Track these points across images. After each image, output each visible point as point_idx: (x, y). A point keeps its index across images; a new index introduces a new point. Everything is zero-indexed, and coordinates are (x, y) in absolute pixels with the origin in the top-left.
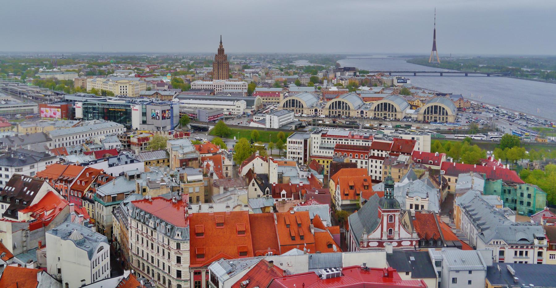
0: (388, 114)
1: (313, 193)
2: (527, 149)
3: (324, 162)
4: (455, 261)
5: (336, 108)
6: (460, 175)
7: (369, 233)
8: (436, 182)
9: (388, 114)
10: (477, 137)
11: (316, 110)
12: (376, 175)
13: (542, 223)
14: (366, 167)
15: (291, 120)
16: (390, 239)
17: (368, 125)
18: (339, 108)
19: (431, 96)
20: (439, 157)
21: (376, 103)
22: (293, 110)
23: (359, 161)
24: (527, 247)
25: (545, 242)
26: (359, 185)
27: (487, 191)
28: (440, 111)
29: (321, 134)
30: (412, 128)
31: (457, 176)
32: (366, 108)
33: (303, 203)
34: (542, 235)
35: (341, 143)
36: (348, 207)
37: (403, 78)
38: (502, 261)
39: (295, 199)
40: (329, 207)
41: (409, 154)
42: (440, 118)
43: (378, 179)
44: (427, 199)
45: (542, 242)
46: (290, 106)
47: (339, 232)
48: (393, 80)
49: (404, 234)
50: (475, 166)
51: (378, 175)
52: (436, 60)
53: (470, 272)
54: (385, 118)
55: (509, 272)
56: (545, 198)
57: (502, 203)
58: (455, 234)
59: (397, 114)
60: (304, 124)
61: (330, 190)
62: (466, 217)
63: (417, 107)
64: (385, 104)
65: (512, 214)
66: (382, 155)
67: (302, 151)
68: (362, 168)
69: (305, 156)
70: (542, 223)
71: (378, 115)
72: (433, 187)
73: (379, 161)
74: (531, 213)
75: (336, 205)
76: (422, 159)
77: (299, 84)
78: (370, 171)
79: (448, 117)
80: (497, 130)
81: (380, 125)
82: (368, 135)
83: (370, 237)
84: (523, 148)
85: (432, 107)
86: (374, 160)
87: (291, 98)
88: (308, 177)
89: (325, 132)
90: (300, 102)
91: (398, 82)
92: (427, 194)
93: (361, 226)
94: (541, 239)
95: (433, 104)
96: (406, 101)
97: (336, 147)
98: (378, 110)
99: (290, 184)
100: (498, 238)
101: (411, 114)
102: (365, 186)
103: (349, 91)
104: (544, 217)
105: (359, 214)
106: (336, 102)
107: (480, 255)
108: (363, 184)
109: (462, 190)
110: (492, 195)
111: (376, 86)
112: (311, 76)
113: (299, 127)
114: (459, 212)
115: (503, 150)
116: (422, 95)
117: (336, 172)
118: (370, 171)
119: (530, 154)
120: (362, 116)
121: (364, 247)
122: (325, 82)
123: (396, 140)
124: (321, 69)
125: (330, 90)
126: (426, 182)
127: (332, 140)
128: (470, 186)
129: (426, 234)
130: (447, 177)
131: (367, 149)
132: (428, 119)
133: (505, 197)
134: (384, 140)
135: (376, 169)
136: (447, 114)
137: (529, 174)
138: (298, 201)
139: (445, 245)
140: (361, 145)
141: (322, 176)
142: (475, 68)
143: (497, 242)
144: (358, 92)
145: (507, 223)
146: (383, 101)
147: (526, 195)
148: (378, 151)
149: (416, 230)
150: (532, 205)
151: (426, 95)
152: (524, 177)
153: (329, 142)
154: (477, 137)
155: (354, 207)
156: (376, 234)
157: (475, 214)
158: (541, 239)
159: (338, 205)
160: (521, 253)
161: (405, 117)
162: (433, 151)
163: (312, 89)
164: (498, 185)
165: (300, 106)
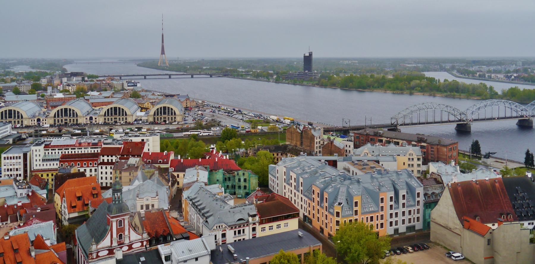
0: (118, 118)
1: (34, 212)
2: (243, 140)
3: (48, 175)
4: (183, 252)
5: (62, 115)
6: (187, 170)
7: (97, 242)
8: (166, 179)
9: (118, 118)
10: (204, 133)
11: (39, 120)
12: (106, 181)
13: (255, 202)
14: (96, 175)
15: (8, 133)
16: (121, 244)
17: (97, 131)
18: (66, 115)
19: (160, 97)
20: (168, 156)
21: (105, 108)
22: (10, 122)
23: (88, 169)
24: (244, 226)
25: (257, 218)
26: (88, 194)
27: (210, 182)
28: (169, 112)
29: (43, 145)
30: (143, 130)
31: (184, 171)
32: (96, 114)
33: (22, 224)
34: (255, 213)
35: (67, 153)
36: (77, 220)
37: (133, 81)
38: (224, 242)
39: (11, 222)
40: (53, 224)
41: (139, 156)
42: (168, 118)
43: (109, 185)
44: (157, 197)
45: (255, 218)
46: (6, 117)
47: (65, 248)
48: (123, 84)
49: (134, 236)
50: (200, 160)
51: (109, 181)
52: (164, 63)
53: (197, 259)
54: (116, 122)
55: (229, 251)
56: (257, 180)
57: (223, 190)
58: (183, 226)
59: (127, 117)
60: (24, 136)
61: (55, 205)
62: (192, 208)
63: (147, 109)
64: (115, 108)
65: (231, 199)
66: (112, 160)
67: (22, 166)
68: (91, 176)
69: (25, 171)
70: (255, 202)
71: (108, 120)
72: (163, 185)
73: (109, 167)
74: (247, 194)
75: (63, 220)
76: (152, 159)
77: (17, 92)
78: (100, 178)
79: (176, 117)
80: (219, 125)
81: (111, 130)
82: (96, 141)
83: (99, 247)
84: (239, 139)
85: (161, 108)
86: (104, 167)
87: (7, 108)
88: (28, 195)
89: (48, 143)
90: (18, 112)
91: (128, 86)
92: (157, 192)
93: (90, 237)
94: (254, 216)
95: (162, 105)
96: (136, 104)
97: (61, 158)
98: (108, 115)
99: (6, 206)
100: (220, 223)
101: (141, 116)
102: (93, 195)
103: (77, 97)
104: (256, 197)
105: (87, 224)
106: (62, 110)
107: (205, 241)
108: (92, 193)
109: (189, 184)
110: (215, 184)
111: (106, 90)
112: (32, 82)
113: (18, 140)
114: (187, 205)
115: (223, 142)
116: (152, 97)
117: (61, 184)
118: (100, 178)
119: (246, 143)
120: (91, 122)
121: (93, 259)
122: (50, 89)
123: (126, 143)
124: (44, 75)
125: (55, 97)
126: (156, 181)
127: (57, 151)
128: (196, 180)
129: (157, 232)
130: (175, 174)
131: (95, 156)
132: (158, 120)
133: (226, 184)
134: (114, 144)
135: (106, 176)
136: (175, 114)
137: (245, 161)
138: (15, 223)
139: (174, 239)
140: (89, 152)
141: (45, 191)
142: (200, 70)
143: (219, 227)
144: (86, 97)
145: (227, 208)
146: (113, 106)
147: (242, 180)
148: (108, 156)
149: (147, 230)
150: (247, 188)
151: (155, 97)
152: (241, 165)
153: (54, 153)
154: (204, 133)
155: (82, 219)
156: (106, 242)
157: (201, 205)
158: (254, 216)
159: (65, 219)
160: (239, 232)
161: (136, 120)
162: (162, 150)
163: (34, 97)
164: (219, 175)
165: (18, 117)
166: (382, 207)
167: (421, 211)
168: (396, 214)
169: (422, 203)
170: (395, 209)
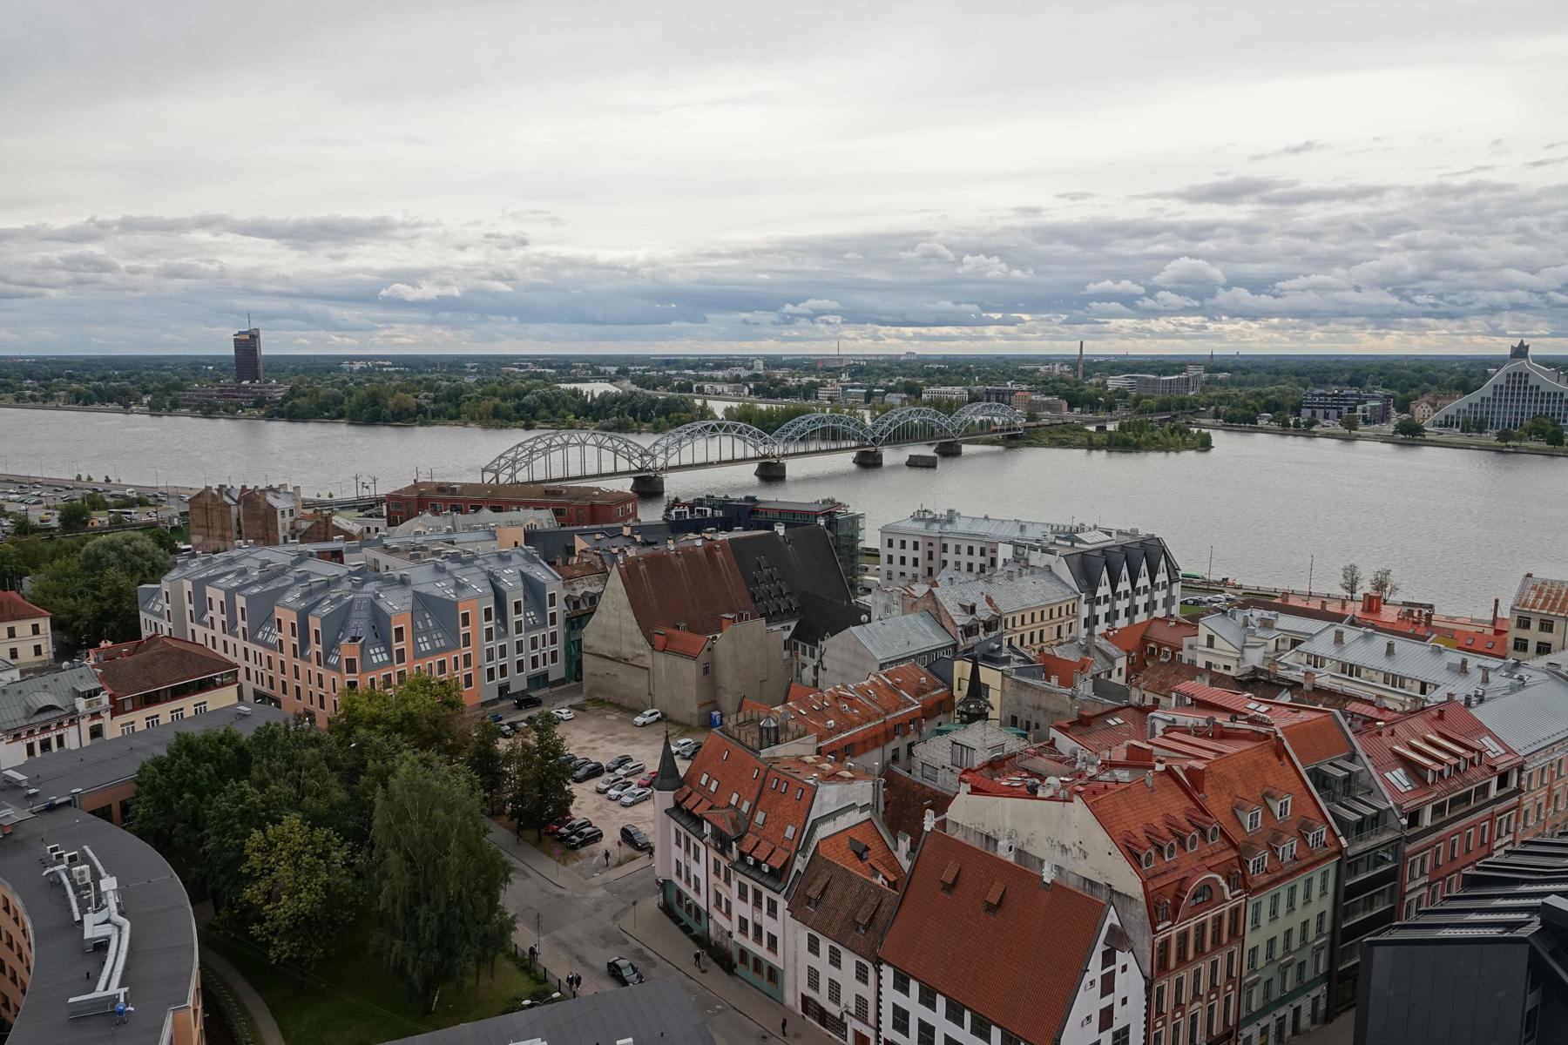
166: (467, 636)
167: (560, 638)
168: (503, 649)
169: (560, 620)
170: (499, 637)
